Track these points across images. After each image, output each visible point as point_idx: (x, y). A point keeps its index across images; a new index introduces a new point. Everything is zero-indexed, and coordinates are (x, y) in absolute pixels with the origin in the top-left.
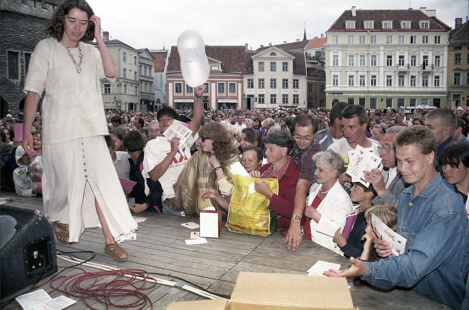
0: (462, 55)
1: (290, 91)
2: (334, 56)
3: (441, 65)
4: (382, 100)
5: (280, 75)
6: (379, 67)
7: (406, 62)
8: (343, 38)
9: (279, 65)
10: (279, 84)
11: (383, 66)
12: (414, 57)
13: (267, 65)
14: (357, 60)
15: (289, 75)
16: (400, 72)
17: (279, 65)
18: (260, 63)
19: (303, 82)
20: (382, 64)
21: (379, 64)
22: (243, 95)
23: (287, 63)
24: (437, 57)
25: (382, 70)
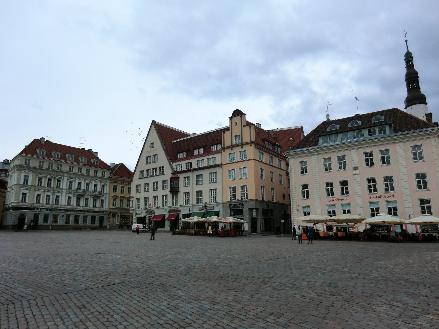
4: (63, 216)
11: (65, 188)
14: (45, 183)
16: (79, 195)
20: (65, 187)
21: (62, 186)
24: (103, 187)
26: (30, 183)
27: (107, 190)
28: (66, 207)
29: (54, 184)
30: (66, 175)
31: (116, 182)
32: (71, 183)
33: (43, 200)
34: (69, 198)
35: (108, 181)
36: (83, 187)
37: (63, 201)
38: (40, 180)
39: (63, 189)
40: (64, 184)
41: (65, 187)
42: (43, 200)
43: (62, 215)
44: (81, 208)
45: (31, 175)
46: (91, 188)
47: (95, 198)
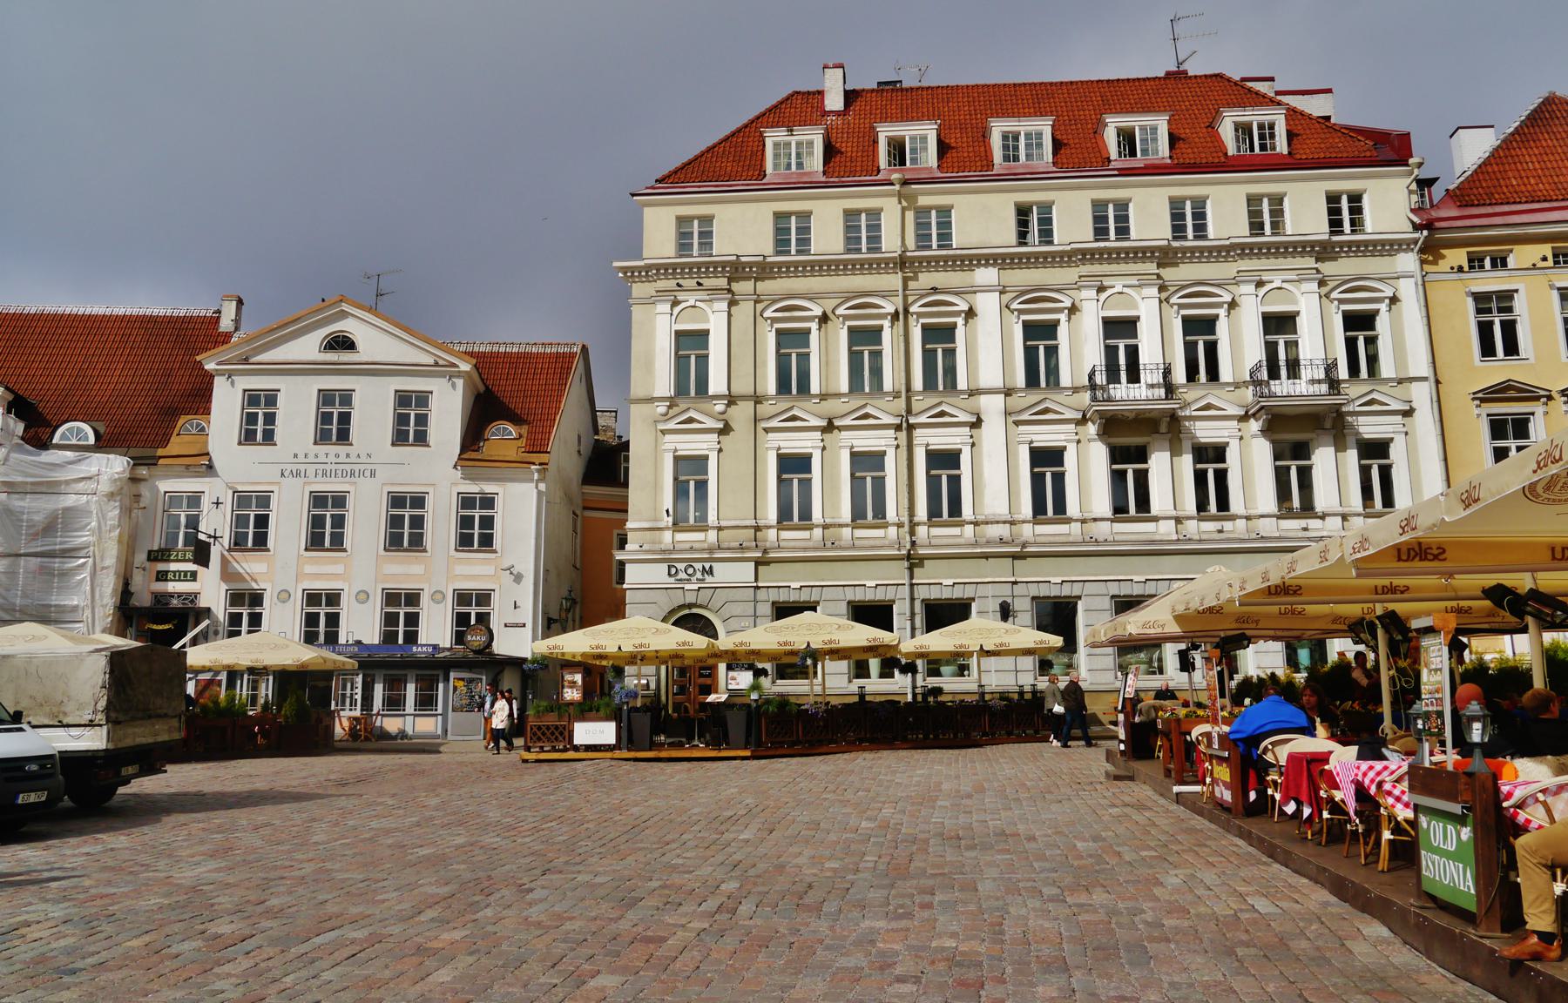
0: (1520, 304)
1: (440, 572)
2: (679, 334)
3: (1387, 369)
5: (374, 469)
6: (973, 393)
7: (1149, 355)
8: (743, 227)
9: (373, 409)
10: (366, 522)
11: (999, 383)
12: (1199, 326)
13: (297, 408)
14: (829, 359)
15: (436, 469)
17: (373, 409)
18: (252, 398)
19: (521, 507)
20: (990, 375)
22: (126, 593)
23: (423, 399)
24: (1359, 322)
25: (992, 406)
26: (717, 383)
27: (1403, 340)
28: (1027, 531)
29: (899, 356)
30: (986, 275)
31: (1500, 262)
32: (1040, 333)
33: (832, 494)
34: (1047, 458)
35: (1408, 261)
36: (1159, 344)
37: (996, 483)
38: (791, 339)
39: (973, 393)
40: (989, 350)
41: (990, 375)
42: (832, 494)
43: (994, 606)
44: (1166, 529)
45: (714, 320)
46: (1241, 344)
47: (1294, 433)
